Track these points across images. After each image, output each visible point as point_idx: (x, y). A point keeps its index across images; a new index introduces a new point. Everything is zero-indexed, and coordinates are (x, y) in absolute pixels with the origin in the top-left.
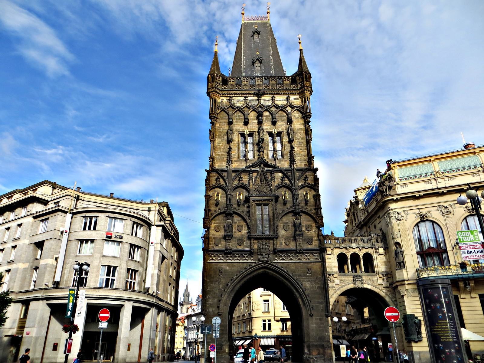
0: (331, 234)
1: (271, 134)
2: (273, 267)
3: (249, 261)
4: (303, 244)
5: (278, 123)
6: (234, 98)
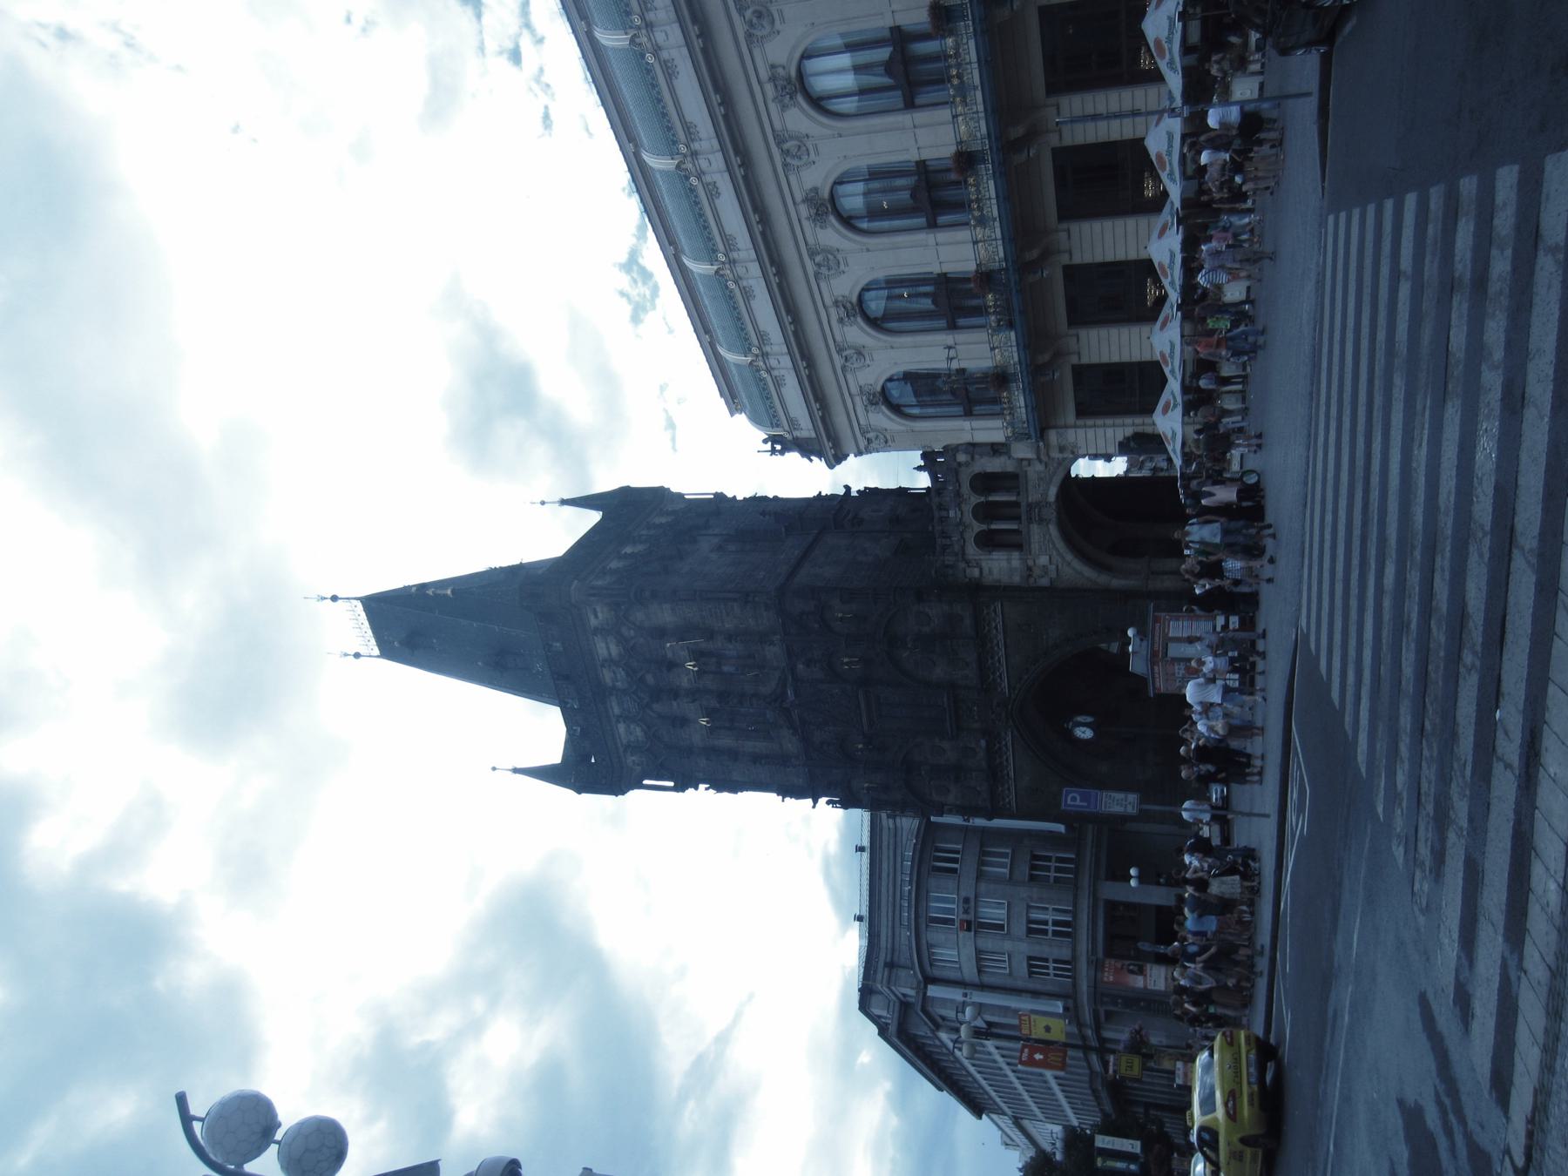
1: (701, 673)
3: (1009, 738)
5: (670, 655)
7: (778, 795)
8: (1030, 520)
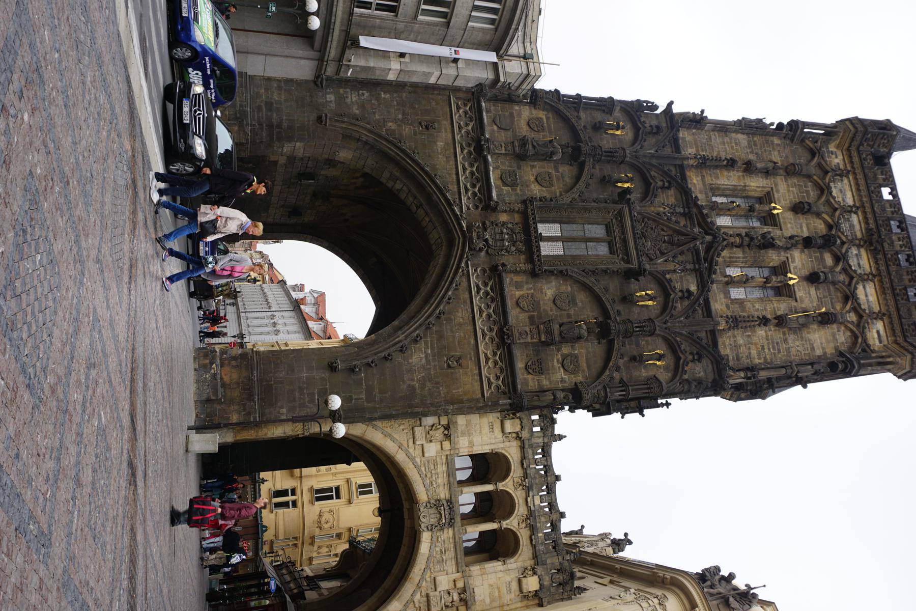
0: (559, 435)
1: (782, 270)
2: (454, 262)
3: (464, 200)
4: (527, 344)
5: (813, 290)
6: (846, 181)
7: (706, 117)
8: (450, 501)
